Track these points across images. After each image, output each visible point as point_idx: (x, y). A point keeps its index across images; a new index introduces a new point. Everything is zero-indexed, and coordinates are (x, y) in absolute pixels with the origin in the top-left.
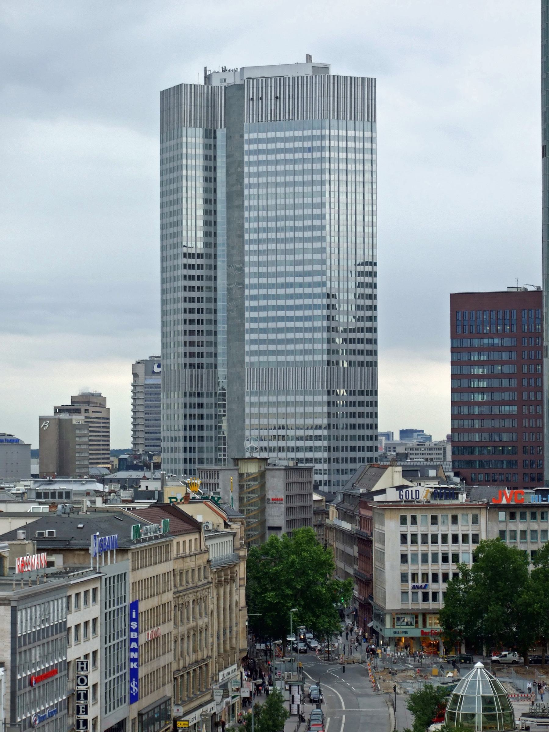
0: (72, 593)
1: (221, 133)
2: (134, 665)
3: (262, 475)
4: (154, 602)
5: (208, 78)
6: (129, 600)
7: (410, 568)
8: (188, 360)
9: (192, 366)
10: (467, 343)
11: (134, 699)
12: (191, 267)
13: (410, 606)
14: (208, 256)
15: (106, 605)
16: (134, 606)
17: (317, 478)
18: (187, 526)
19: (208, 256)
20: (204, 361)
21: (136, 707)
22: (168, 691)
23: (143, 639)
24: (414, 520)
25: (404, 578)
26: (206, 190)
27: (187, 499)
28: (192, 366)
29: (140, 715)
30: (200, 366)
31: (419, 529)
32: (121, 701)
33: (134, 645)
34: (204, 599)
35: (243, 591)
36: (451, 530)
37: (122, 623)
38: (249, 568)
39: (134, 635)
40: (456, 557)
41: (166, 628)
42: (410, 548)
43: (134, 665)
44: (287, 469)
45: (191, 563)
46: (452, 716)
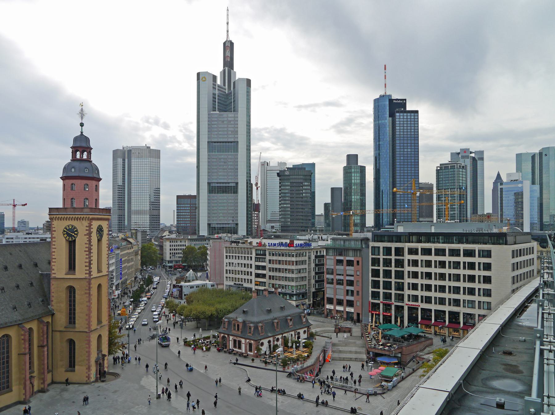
0: (110, 257)
2: (121, 272)
3: (136, 233)
7: (172, 251)
8: (119, 208)
9: (119, 209)
10: (180, 206)
11: (121, 279)
12: (119, 188)
13: (171, 259)
14: (123, 186)
17: (147, 233)
19: (123, 186)
23: (123, 266)
25: (170, 254)
26: (123, 172)
27: (127, 238)
28: (119, 209)
29: (122, 282)
30: (121, 209)
31: (174, 244)
32: (118, 280)
33: (121, 268)
35: (140, 257)
36: (180, 244)
39: (121, 266)
42: (172, 248)
43: (121, 272)
44: (142, 231)
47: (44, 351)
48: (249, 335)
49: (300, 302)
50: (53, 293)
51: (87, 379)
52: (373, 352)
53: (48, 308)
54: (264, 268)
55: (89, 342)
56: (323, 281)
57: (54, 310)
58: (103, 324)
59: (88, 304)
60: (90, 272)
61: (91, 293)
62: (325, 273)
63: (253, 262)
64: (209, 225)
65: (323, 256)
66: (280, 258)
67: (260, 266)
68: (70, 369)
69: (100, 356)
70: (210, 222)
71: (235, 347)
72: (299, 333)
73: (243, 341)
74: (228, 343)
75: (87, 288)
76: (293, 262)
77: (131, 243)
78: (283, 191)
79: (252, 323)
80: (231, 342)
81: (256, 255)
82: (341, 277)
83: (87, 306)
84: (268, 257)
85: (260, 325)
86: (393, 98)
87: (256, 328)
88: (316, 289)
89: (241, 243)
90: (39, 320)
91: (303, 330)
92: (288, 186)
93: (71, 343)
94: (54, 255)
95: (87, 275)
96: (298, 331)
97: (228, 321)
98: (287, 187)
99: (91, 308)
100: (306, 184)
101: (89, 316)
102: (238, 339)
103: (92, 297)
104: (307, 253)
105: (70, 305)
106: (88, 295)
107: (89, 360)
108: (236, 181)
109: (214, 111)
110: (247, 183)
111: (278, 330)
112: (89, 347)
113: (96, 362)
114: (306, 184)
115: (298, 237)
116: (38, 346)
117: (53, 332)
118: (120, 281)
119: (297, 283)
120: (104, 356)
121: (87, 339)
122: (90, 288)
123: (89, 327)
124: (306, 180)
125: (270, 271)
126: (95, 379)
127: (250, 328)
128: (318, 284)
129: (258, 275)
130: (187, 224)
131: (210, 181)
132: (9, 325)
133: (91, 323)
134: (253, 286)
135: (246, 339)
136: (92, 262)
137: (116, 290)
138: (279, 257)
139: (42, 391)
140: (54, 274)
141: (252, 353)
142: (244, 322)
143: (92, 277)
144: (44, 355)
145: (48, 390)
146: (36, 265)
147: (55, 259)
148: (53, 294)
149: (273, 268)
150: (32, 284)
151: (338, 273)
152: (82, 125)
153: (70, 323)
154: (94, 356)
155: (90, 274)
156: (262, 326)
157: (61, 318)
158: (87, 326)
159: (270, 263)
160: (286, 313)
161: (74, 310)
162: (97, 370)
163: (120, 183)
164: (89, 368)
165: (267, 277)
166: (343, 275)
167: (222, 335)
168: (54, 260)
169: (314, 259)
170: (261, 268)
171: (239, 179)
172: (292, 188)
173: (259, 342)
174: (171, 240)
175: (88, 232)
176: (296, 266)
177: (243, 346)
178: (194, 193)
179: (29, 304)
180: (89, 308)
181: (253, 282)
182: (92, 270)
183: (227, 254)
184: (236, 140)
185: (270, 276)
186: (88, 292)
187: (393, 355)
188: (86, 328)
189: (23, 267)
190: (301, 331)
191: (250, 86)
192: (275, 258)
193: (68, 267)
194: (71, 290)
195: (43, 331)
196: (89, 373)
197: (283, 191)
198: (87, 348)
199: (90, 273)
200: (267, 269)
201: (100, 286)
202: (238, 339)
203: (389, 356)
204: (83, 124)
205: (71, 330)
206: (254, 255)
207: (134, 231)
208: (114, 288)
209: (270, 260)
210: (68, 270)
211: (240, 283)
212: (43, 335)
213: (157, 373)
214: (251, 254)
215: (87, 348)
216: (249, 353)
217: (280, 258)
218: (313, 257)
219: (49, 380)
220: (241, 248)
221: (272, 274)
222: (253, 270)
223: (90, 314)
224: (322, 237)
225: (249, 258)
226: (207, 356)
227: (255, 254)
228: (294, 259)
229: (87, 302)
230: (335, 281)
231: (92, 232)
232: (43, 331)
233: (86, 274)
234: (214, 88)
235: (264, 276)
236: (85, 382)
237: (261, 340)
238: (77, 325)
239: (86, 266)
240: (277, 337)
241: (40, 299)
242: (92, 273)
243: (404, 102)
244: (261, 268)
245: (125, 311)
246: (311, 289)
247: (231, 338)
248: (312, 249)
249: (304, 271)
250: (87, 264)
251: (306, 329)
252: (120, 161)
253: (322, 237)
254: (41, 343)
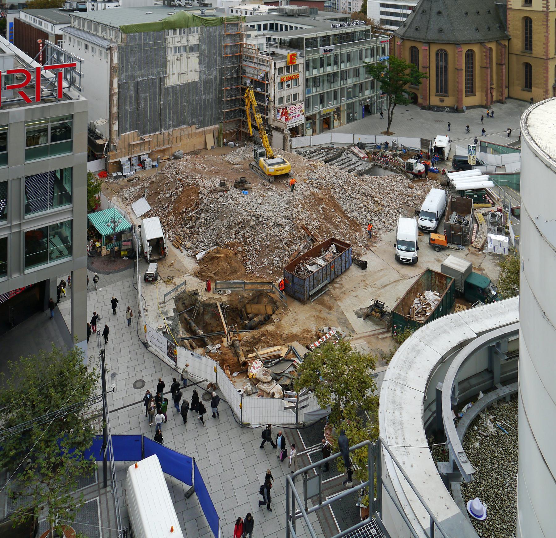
59: (545, 34)
61: (549, 25)
75: (545, 20)
83: (545, 36)
90: (498, 42)
95: (545, 9)
101: (546, 44)
103: (549, 28)
105: (526, 33)
106: (545, 26)
123: (547, 55)
132: (473, 42)
139: (501, 102)
143: (549, 10)
145: (506, 103)
153: (526, 48)
158: (545, 54)
161: (531, 38)
180: (547, 38)
198: (544, 73)
199: (547, 7)
205: (528, 55)
212: (502, 55)
219: (506, 95)
233: (543, 7)
238: (533, 52)
242: (549, 7)
254: (499, 62)
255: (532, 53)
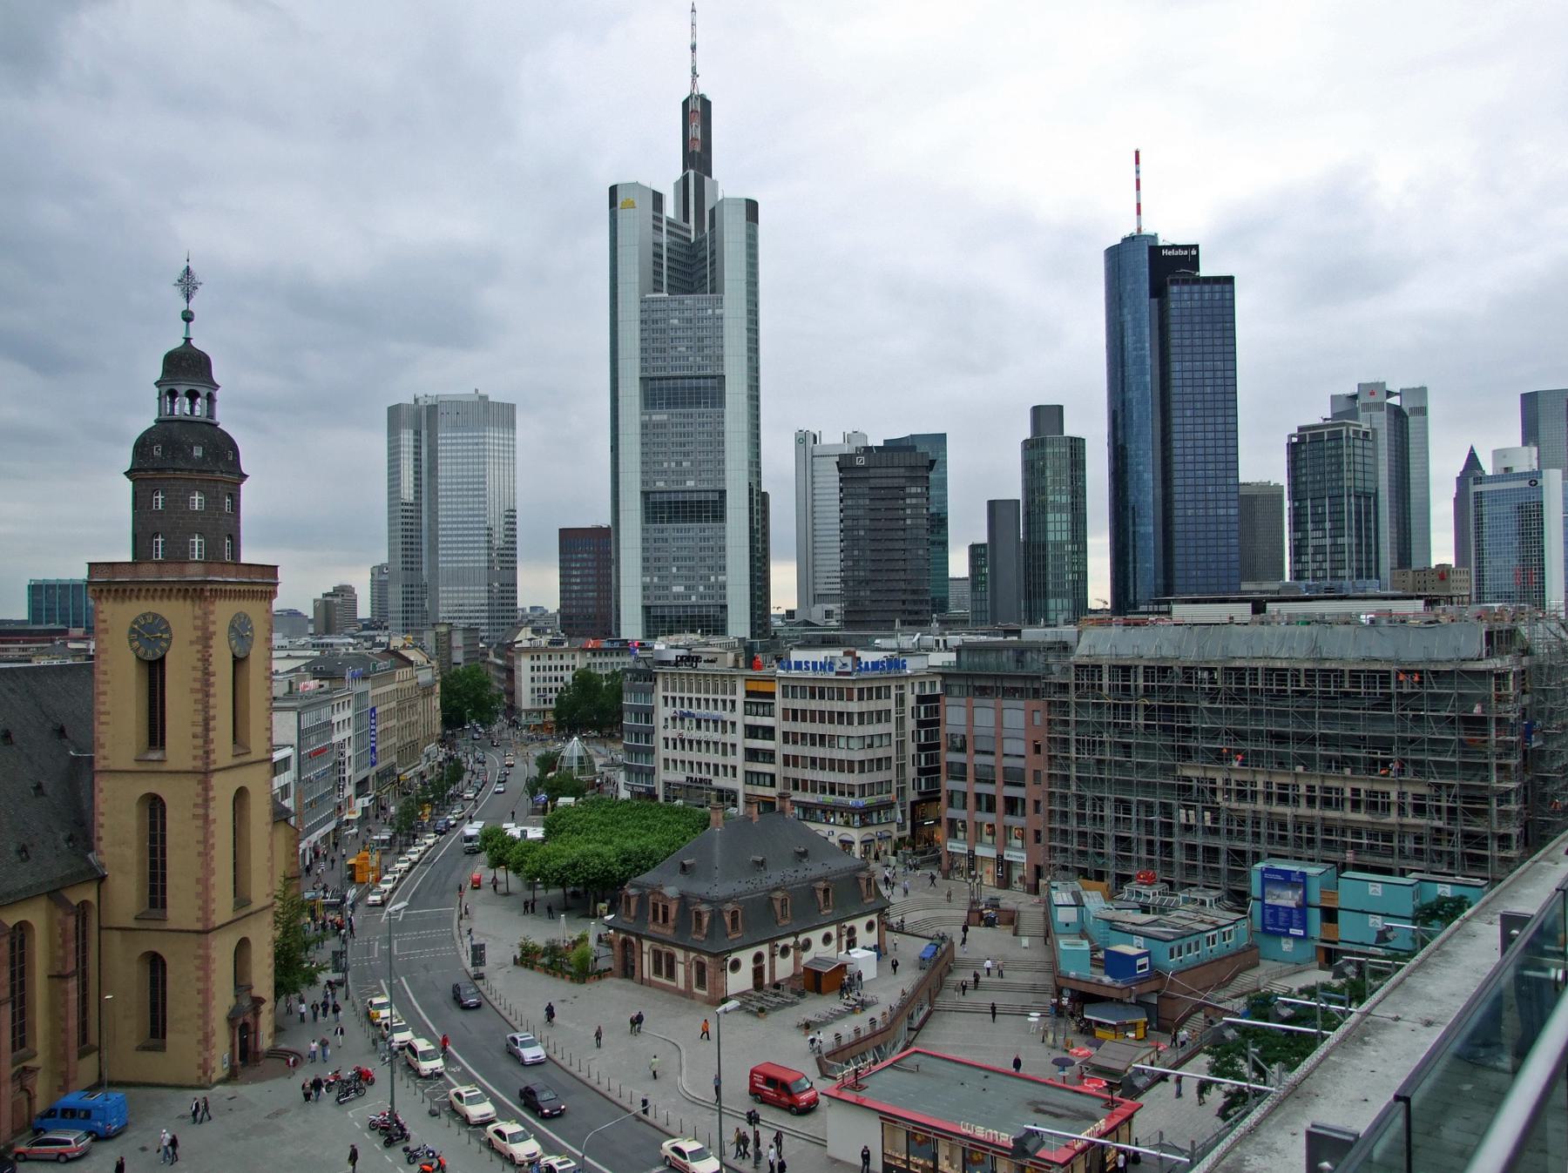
0: (335, 703)
1: (424, 433)
3: (449, 633)
4: (385, 707)
5: (416, 400)
6: (370, 707)
7: (536, 685)
10: (568, 556)
11: (373, 764)
12: (407, 511)
13: (536, 707)
15: (356, 710)
16: (373, 710)
17: (482, 634)
18: (403, 663)
20: (414, 566)
21: (375, 769)
22: (394, 759)
24: (538, 657)
25: (533, 691)
26: (415, 466)
27: (404, 647)
31: (541, 663)
32: (366, 765)
34: (415, 705)
35: (438, 701)
36: (559, 663)
37: (366, 720)
38: (442, 687)
40: (562, 678)
41: (393, 722)
42: (536, 674)
44: (464, 629)
45: (407, 684)
46: (560, 768)
47: (66, 993)
48: (695, 937)
49: (872, 830)
50: (103, 814)
51: (200, 1072)
52: (1072, 990)
53: (89, 862)
54: (768, 733)
55: (205, 962)
56: (937, 770)
57: (103, 866)
58: (254, 907)
60: (207, 753)
61: (211, 817)
62: (943, 750)
63: (740, 717)
64: (647, 609)
65: (936, 698)
66: (815, 705)
67: (757, 727)
68: (154, 1041)
69: (246, 1003)
70: (648, 603)
71: (658, 971)
72: (852, 931)
73: (680, 955)
74: (637, 960)
75: (200, 801)
76: (850, 715)
77: (410, 663)
78: (849, 512)
79: (704, 901)
80: (645, 957)
81: (749, 694)
82: (989, 760)
83: (200, 854)
84: (779, 703)
85: (730, 907)
86: (1161, 243)
87: (717, 916)
88: (919, 793)
89: (707, 661)
91: (865, 921)
92: (863, 496)
93: (156, 963)
94: (104, 703)
96: (848, 924)
97: (640, 896)
98: (861, 502)
99: (212, 858)
100: (913, 490)
101: (204, 884)
102: (665, 949)
104: (893, 688)
106: (200, 823)
107: (205, 1016)
108: (720, 487)
109: (656, 291)
110: (751, 491)
111: (786, 922)
112: (206, 978)
113: (231, 1020)
114: (913, 490)
115: (877, 641)
116: (50, 977)
117: (103, 932)
118: (371, 772)
119: (864, 775)
120: (258, 1002)
121: (201, 952)
122: (206, 802)
123: (206, 918)
124: (913, 480)
125: (786, 741)
126: (227, 1072)
127: (699, 914)
128: (927, 780)
129: (752, 755)
130: (587, 607)
131: (647, 489)
133: (213, 906)
134: (738, 784)
135: (687, 949)
136: (212, 723)
137: (358, 796)
138: (813, 701)
140: (105, 758)
141: (705, 993)
142: (683, 899)
144: (66, 1001)
146: (61, 732)
147: (109, 713)
148: (101, 819)
149: (795, 734)
150: (39, 787)
151: (978, 748)
152: (188, 317)
154: (223, 999)
155: (208, 758)
156: (735, 913)
157: (126, 892)
158: (200, 914)
159: (785, 718)
160: (815, 869)
162: (233, 1046)
163: (407, 493)
164: (206, 1041)
165: (779, 758)
166: (992, 753)
167: (622, 936)
168: (103, 718)
169: (915, 704)
170: (760, 732)
171: (727, 482)
172: (877, 503)
173: (726, 960)
174: (535, 652)
175: (199, 633)
176: (860, 727)
177: (680, 970)
178: (605, 521)
179: (23, 851)
181: (740, 772)
182: (212, 746)
183: (666, 694)
184: (718, 372)
185: (786, 757)
186: (201, 811)
187: (1133, 1000)
188: (198, 920)
189: (15, 737)
190: (860, 924)
191: (756, 221)
192: (799, 704)
193: (145, 739)
194: (154, 806)
195: (64, 930)
196: (207, 1055)
197: (849, 512)
198: (198, 979)
200: (778, 735)
201: (241, 795)
202: (665, 949)
203: (1120, 1001)
204: (192, 313)
205: (154, 925)
206: (740, 697)
207: (443, 629)
208: (350, 790)
209: (785, 710)
210: (146, 745)
211: (704, 775)
213: (391, 1061)
214: (734, 692)
215: (198, 979)
216: (696, 990)
217: (815, 705)
218: (911, 701)
220: (705, 675)
221: (791, 749)
222: (738, 738)
223: (207, 879)
224: (945, 641)
225: (729, 705)
226: (574, 1000)
227: (744, 694)
228: (854, 707)
229: (198, 842)
230: (970, 770)
231: (214, 633)
232: (64, 930)
234: (658, 229)
235: (769, 756)
236: (195, 1083)
237: (730, 952)
238: (170, 911)
239: (195, 736)
240: (781, 943)
241: (62, 835)
242: (213, 757)
243: (1194, 252)
244: (760, 732)
245: (366, 858)
246: (907, 792)
247: (647, 945)
248: (907, 677)
249: (885, 741)
250: (199, 730)
251: (874, 917)
252: (407, 437)
253: (945, 641)
255: (164, 919)
